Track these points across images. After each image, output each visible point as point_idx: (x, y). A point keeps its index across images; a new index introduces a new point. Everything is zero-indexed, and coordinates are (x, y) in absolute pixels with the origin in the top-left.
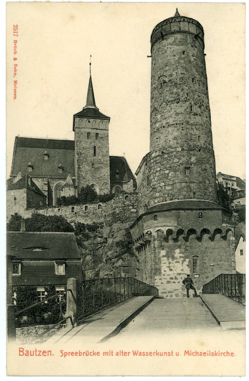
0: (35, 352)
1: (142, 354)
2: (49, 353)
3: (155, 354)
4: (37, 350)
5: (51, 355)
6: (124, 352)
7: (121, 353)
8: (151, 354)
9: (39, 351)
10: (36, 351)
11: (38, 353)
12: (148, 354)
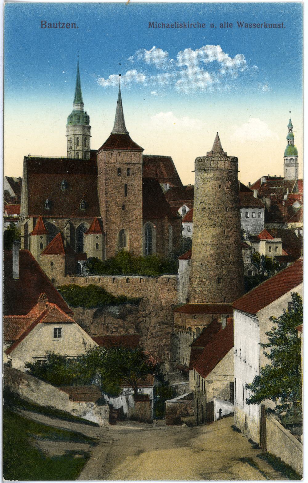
0: (58, 24)
1: (249, 26)
2: (73, 25)
3: (263, 26)
4: (61, 22)
5: (75, 27)
6: (229, 23)
7: (226, 25)
8: (258, 26)
9: (62, 24)
10: (59, 23)
11: (61, 26)
12: (256, 25)
